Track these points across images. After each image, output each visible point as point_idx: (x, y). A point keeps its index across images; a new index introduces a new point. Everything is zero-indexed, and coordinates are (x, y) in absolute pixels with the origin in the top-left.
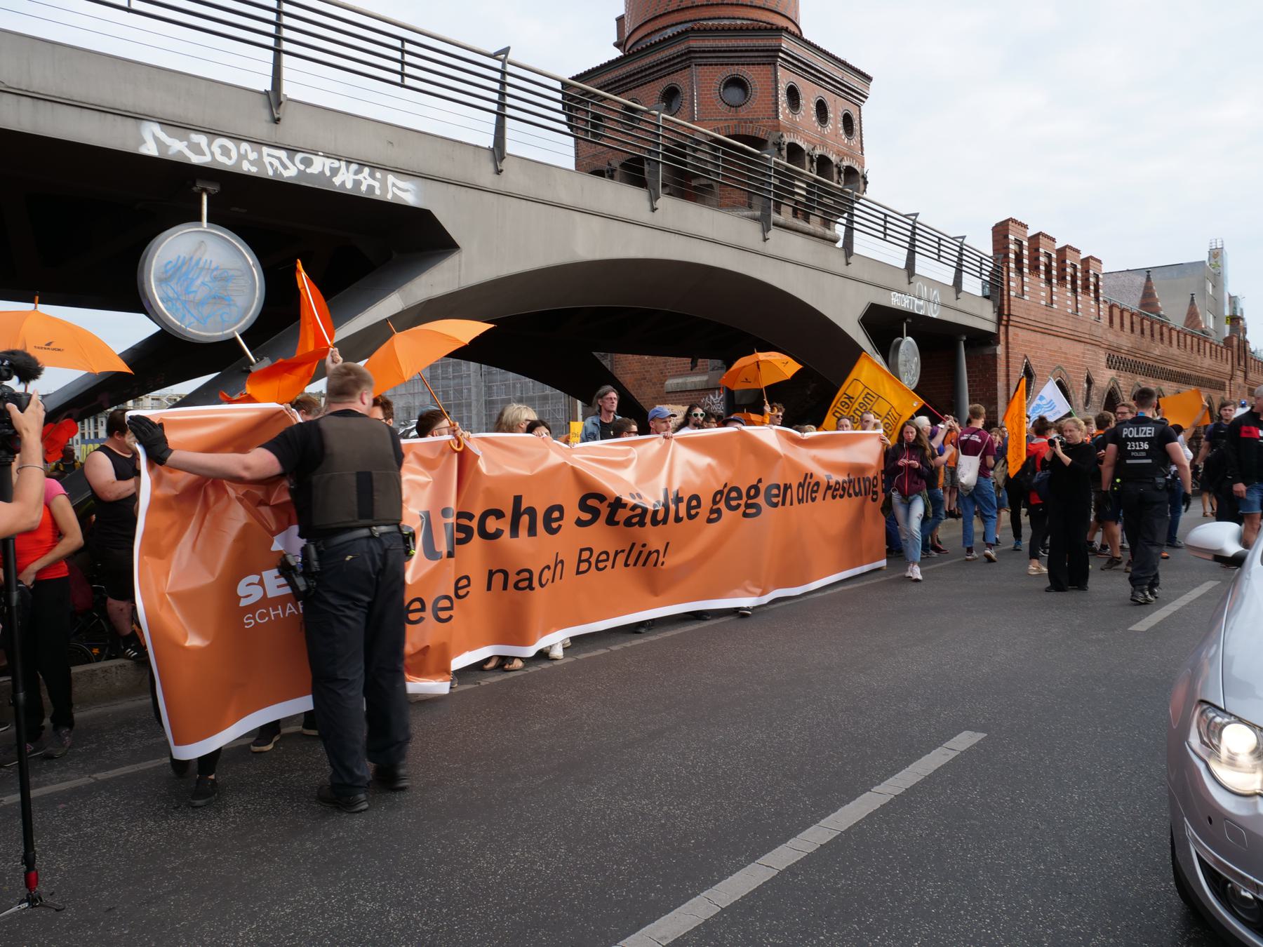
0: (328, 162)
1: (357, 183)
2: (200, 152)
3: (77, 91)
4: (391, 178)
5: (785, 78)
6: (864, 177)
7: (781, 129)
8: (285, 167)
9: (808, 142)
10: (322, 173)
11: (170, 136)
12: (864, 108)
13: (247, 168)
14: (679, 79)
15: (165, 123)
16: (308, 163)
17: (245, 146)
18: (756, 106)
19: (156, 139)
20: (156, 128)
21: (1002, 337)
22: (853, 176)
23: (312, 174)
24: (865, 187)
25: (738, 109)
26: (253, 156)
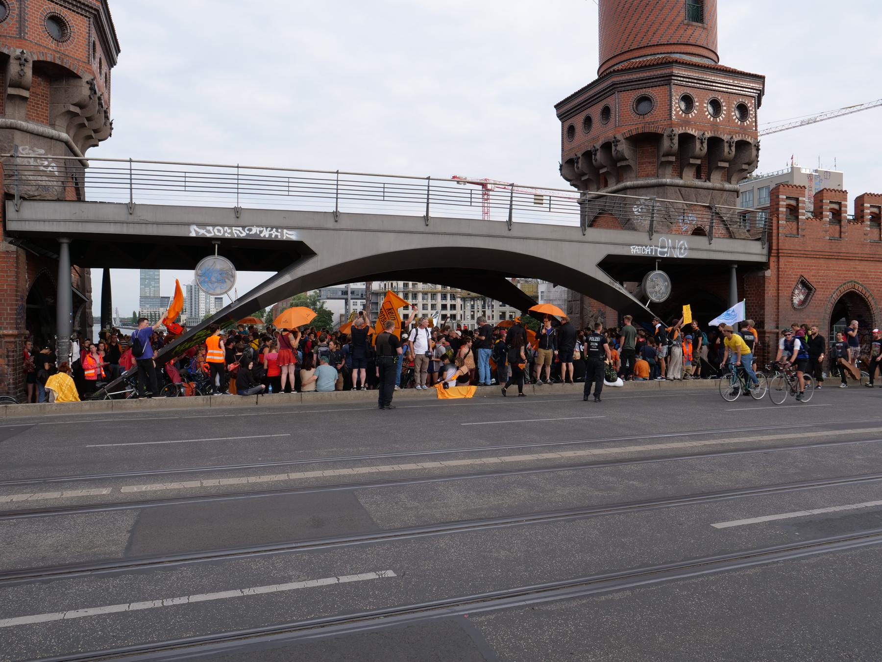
0: (258, 229)
3: (170, 219)
4: (285, 231)
8: (241, 233)
10: (256, 233)
14: (610, 101)
15: (198, 225)
16: (250, 230)
17: (226, 228)
19: (195, 231)
20: (195, 227)
21: (773, 264)
23: (252, 234)
24: (758, 153)
26: (229, 231)
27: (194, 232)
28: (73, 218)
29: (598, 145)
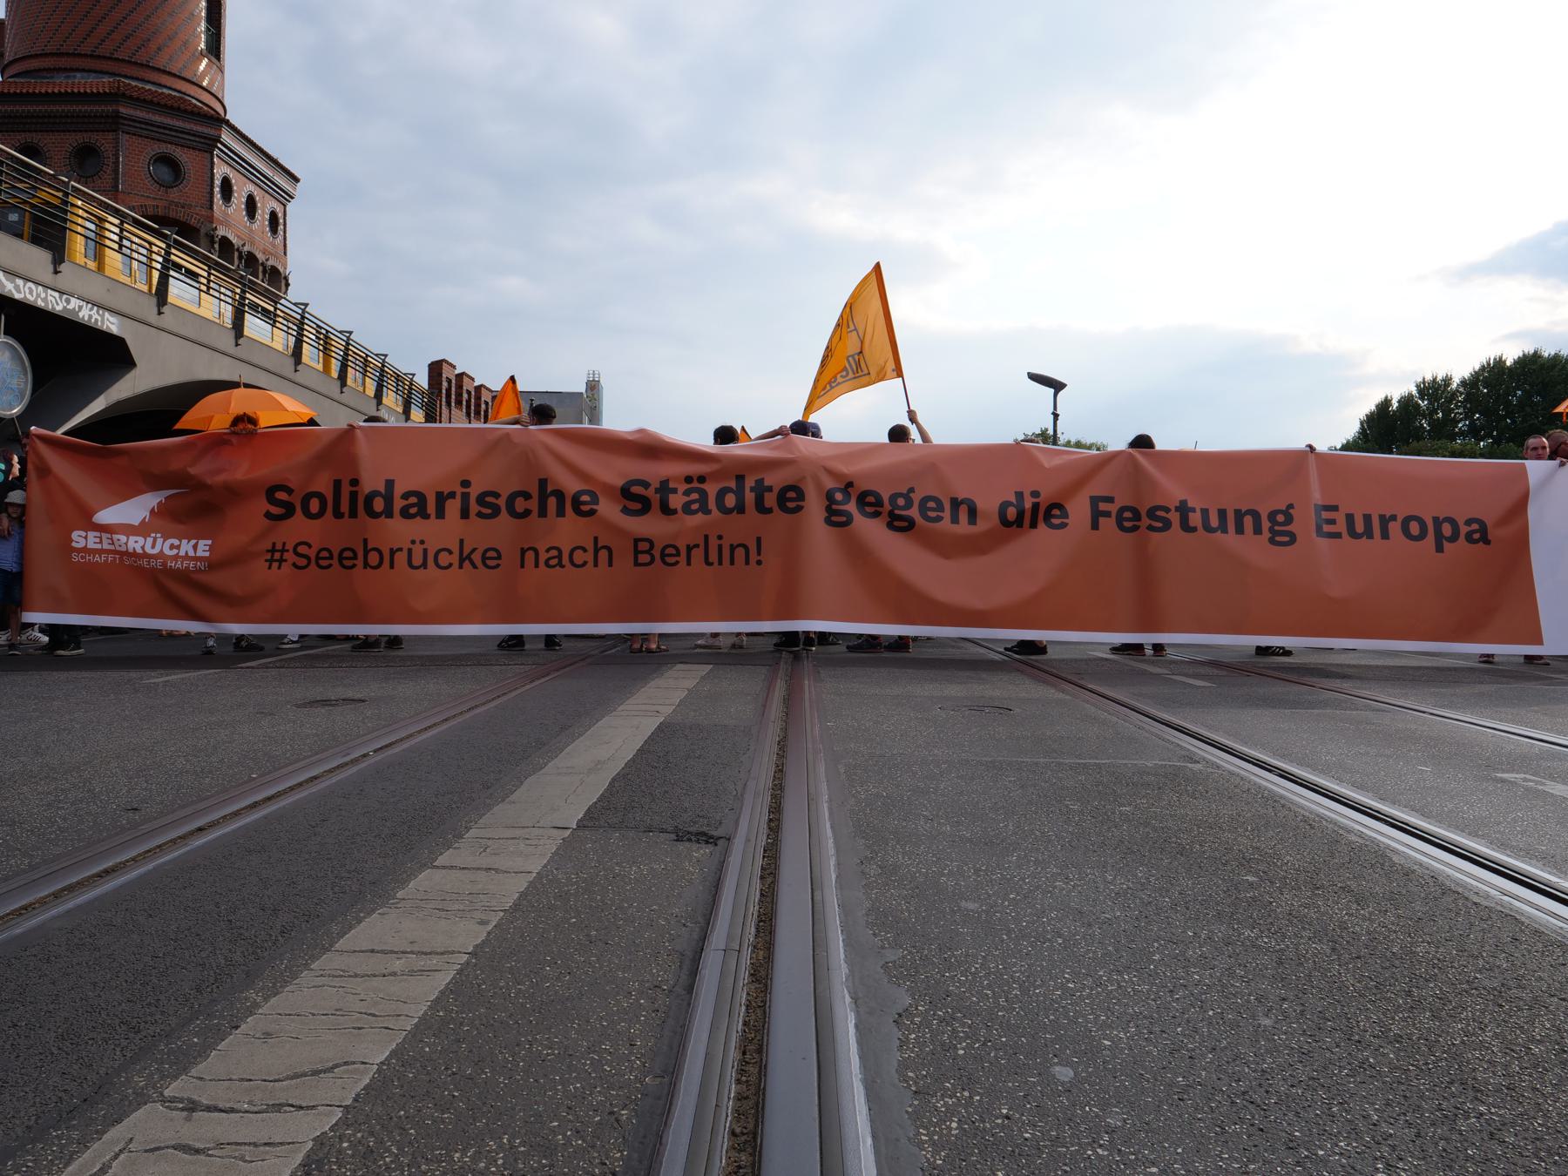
0: (78, 301)
1: (90, 316)
2: (19, 292)
5: (221, 170)
6: (286, 279)
7: (215, 221)
8: (58, 304)
9: (238, 237)
10: (74, 309)
11: (7, 280)
13: (40, 303)
14: (102, 141)
16: (68, 301)
17: (40, 288)
22: (277, 278)
24: (287, 289)
25: (169, 190)
26: (43, 295)
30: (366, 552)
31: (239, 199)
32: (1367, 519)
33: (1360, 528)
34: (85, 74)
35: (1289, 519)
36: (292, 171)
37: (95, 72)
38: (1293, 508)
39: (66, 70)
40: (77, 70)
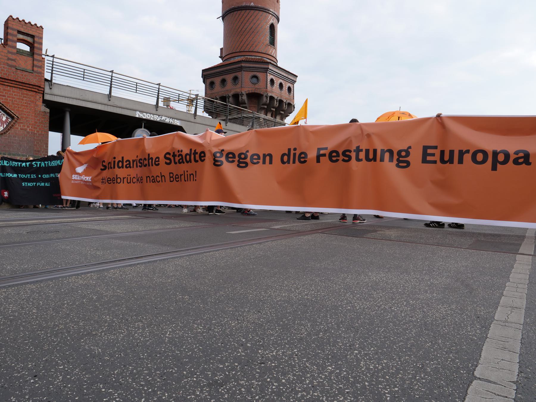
0: (165, 117)
1: (170, 121)
2: (144, 116)
3: (128, 106)
4: (175, 120)
5: (270, 77)
6: (294, 106)
7: (268, 92)
8: (158, 119)
10: (164, 119)
12: (295, 85)
13: (152, 119)
14: (238, 74)
15: (140, 111)
16: (161, 118)
17: (152, 115)
18: (261, 84)
19: (138, 114)
20: (138, 112)
24: (294, 109)
26: (153, 117)
27: (138, 115)
28: (81, 98)
29: (230, 94)
30: (117, 179)
31: (277, 85)
32: (452, 152)
33: (447, 158)
34: (238, 57)
35: (408, 154)
36: (294, 74)
37: (240, 56)
38: (411, 148)
39: (233, 57)
40: (236, 56)
